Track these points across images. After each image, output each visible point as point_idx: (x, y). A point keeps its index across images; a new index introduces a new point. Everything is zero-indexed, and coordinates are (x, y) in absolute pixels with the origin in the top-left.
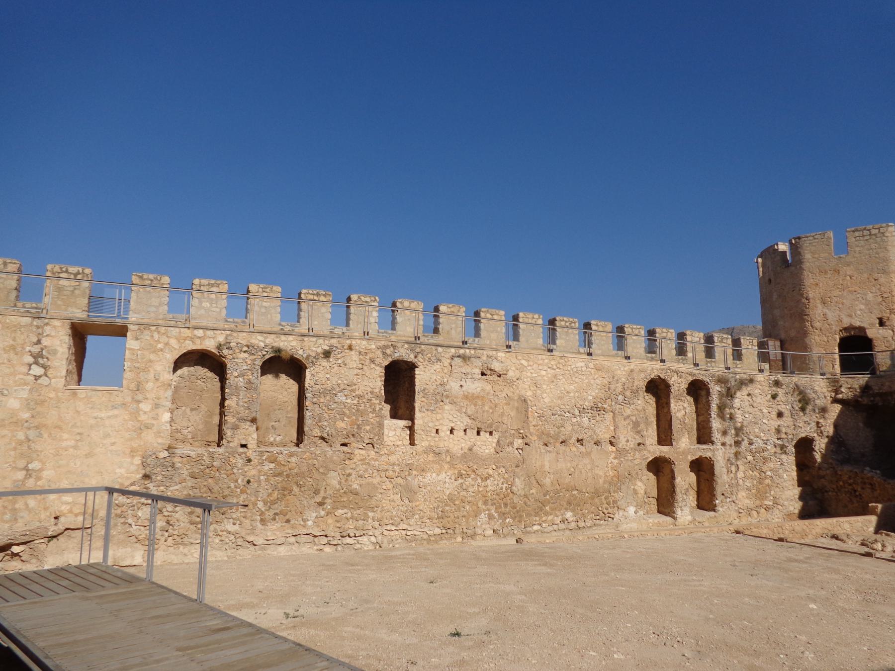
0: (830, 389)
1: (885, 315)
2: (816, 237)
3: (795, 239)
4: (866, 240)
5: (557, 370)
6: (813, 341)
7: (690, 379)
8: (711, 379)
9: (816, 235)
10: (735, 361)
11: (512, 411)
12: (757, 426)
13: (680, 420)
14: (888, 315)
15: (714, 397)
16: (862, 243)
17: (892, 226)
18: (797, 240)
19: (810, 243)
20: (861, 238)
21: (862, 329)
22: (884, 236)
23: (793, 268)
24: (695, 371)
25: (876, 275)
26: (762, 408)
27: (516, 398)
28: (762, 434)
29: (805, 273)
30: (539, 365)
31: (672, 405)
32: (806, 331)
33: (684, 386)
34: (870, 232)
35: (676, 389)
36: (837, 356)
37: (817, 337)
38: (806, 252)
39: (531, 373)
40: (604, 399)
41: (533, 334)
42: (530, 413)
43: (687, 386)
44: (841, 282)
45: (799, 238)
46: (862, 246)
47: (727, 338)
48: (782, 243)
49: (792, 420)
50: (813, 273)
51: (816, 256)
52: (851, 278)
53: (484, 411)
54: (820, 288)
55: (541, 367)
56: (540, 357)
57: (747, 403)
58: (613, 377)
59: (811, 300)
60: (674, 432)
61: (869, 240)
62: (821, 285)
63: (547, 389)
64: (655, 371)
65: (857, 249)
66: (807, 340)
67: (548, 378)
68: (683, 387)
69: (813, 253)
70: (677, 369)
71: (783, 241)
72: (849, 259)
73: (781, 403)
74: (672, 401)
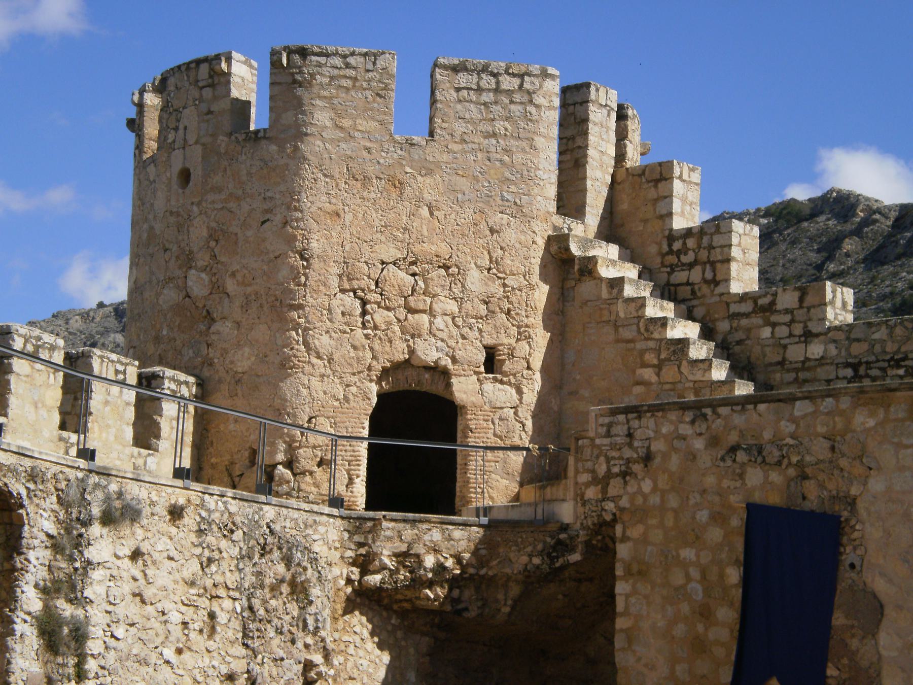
0: (350, 553)
1: (505, 341)
2: (352, 60)
3: (290, 52)
4: (485, 104)
6: (305, 392)
8: (32, 486)
9: (353, 54)
10: (65, 434)
12: (144, 669)
14: (513, 341)
15: (32, 555)
16: (474, 112)
17: (552, 77)
18: (296, 57)
19: (332, 78)
20: (473, 96)
21: (444, 374)
22: (531, 101)
23: (274, 148)
25: (498, 219)
26: (167, 605)
29: (308, 172)
32: (288, 359)
34: (498, 83)
36: (363, 449)
37: (315, 382)
38: (318, 102)
45: (303, 52)
46: (471, 121)
47: (53, 348)
48: (243, 58)
49: (243, 651)
50: (331, 177)
51: (346, 123)
52: (431, 214)
57: (127, 587)
59: (315, 263)
62: (349, 217)
65: (460, 128)
66: (287, 387)
71: (249, 55)
72: (434, 152)
73: (222, 592)
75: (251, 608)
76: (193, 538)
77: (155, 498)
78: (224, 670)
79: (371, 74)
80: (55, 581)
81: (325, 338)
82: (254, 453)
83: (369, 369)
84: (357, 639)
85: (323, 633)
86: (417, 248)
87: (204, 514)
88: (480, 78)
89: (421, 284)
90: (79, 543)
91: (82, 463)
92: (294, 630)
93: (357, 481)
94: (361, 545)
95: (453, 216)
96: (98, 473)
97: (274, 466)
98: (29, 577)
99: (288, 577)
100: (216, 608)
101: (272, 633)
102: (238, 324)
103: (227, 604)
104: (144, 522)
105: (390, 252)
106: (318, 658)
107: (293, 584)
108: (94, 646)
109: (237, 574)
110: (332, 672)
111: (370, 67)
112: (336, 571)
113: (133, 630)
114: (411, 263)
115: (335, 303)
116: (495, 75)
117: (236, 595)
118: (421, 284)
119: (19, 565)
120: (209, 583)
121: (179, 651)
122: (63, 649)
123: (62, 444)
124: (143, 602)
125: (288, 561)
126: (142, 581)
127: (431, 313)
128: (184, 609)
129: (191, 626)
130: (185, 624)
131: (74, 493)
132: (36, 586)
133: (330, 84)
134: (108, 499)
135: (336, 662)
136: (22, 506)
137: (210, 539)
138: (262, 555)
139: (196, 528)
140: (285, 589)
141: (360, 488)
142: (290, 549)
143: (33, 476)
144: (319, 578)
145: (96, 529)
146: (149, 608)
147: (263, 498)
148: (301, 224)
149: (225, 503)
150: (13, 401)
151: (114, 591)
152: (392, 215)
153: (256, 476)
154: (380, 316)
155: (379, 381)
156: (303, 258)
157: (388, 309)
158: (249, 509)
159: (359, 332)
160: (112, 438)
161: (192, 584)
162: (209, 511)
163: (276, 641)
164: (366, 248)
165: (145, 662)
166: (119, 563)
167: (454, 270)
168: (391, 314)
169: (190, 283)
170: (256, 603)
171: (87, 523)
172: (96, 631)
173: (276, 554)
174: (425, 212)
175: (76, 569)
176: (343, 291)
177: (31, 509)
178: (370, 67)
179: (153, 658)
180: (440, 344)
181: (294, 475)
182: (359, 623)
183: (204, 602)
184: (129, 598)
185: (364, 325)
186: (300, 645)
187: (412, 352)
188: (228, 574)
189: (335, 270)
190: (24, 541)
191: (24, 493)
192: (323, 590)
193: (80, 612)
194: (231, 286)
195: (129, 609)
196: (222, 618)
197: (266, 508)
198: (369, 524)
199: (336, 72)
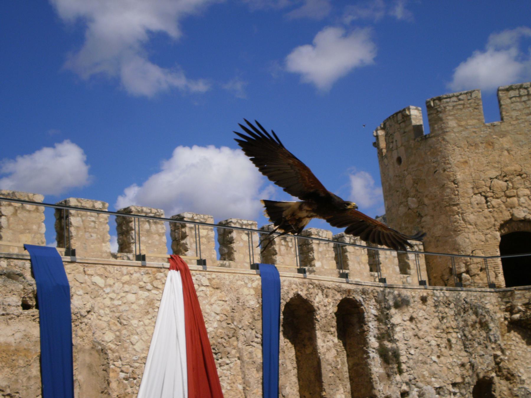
0: (503, 307)
2: (461, 97)
4: (524, 102)
5: (154, 291)
6: (467, 240)
7: (339, 297)
8: (364, 296)
9: (461, 94)
10: (373, 273)
11: (487, 321)
12: (426, 366)
13: (330, 364)
15: (370, 324)
16: (520, 106)
18: (437, 102)
19: (454, 106)
20: (518, 99)
24: (345, 286)
26: (429, 338)
27: (87, 347)
28: (433, 379)
29: (450, 147)
30: (124, 283)
31: (320, 342)
33: (332, 309)
34: (528, 92)
35: (323, 314)
36: (499, 261)
37: (471, 236)
38: (449, 118)
39: (112, 299)
40: (226, 338)
41: (94, 235)
42: (111, 374)
43: (336, 309)
44: (497, 158)
45: (440, 99)
46: (520, 110)
48: (414, 107)
49: (465, 354)
50: (461, 147)
51: (463, 123)
52: (509, 153)
53: (29, 378)
54: (470, 167)
55: (127, 288)
56: (124, 269)
57: (411, 333)
58: (238, 299)
59: (461, 185)
60: (326, 386)
61: (528, 102)
62: (471, 162)
63: (138, 327)
64: (294, 286)
65: (514, 114)
67: (140, 306)
68: (331, 311)
69: (458, 120)
70: (321, 283)
71: (417, 105)
72: (504, 127)
73: (451, 330)
74: (319, 334)
75: (465, 335)
76: (433, 309)
77: (414, 295)
78: (459, 362)
79: (470, 101)
80: (381, 334)
81: (472, 216)
82: (451, 270)
83: (494, 225)
84: (515, 343)
85: (499, 342)
86: (505, 169)
87: (436, 299)
88: (519, 91)
89: (510, 184)
90: (388, 317)
91: (381, 284)
92: (486, 342)
93: (499, 275)
94: (507, 303)
95: (519, 152)
96: (389, 288)
97: (461, 274)
98: (371, 333)
99: (478, 320)
100: (450, 337)
101: (476, 345)
102: (432, 216)
103: (454, 335)
104: (412, 305)
105: (494, 173)
106: (499, 353)
107: (481, 323)
108: (403, 359)
109: (455, 322)
110: (506, 358)
111: (469, 98)
112: (499, 315)
113: (417, 350)
114: (504, 176)
115: (473, 200)
116: (526, 88)
117: (457, 330)
118: (510, 184)
119: (366, 329)
120: (444, 327)
121: (439, 357)
122: (391, 361)
123: (372, 277)
124: (419, 338)
125: (476, 313)
126: (417, 330)
127: (518, 196)
128: (436, 339)
129: (441, 346)
130: (438, 345)
131: (381, 297)
132: (375, 337)
133: (453, 109)
134: (395, 298)
135: (507, 354)
136: (362, 305)
137: (440, 309)
138: (464, 313)
139: (433, 305)
140: (478, 326)
141: (501, 279)
142: (476, 309)
143: (364, 292)
144: (492, 319)
145: (393, 311)
146: (422, 341)
147: (459, 289)
148: (451, 170)
149: (443, 293)
150: (350, 263)
151: (406, 335)
152: (491, 158)
153: (453, 280)
154: (494, 202)
155: (500, 230)
156: (455, 184)
157: (497, 198)
158: (454, 294)
159: (486, 211)
160: (391, 272)
161: (437, 328)
162: (437, 297)
163: (479, 348)
164: (482, 174)
165: (425, 363)
166: (405, 323)
167: (524, 175)
168: (499, 200)
169: (409, 203)
170: (466, 333)
171: (389, 308)
172: (403, 352)
173: (470, 311)
174: (506, 153)
175: (389, 328)
176: (475, 194)
177: (366, 306)
178: (469, 98)
179: (429, 361)
180: (525, 209)
181: (471, 276)
182: (515, 336)
183: (444, 335)
184: (413, 337)
185: (488, 208)
186: (490, 348)
187: (512, 215)
188: (452, 322)
189: (470, 186)
190: (366, 319)
191: (361, 300)
192: (494, 324)
193: (394, 345)
194: (426, 201)
195: (414, 342)
196: (453, 341)
197: (462, 292)
198: (509, 293)
199: (455, 104)
